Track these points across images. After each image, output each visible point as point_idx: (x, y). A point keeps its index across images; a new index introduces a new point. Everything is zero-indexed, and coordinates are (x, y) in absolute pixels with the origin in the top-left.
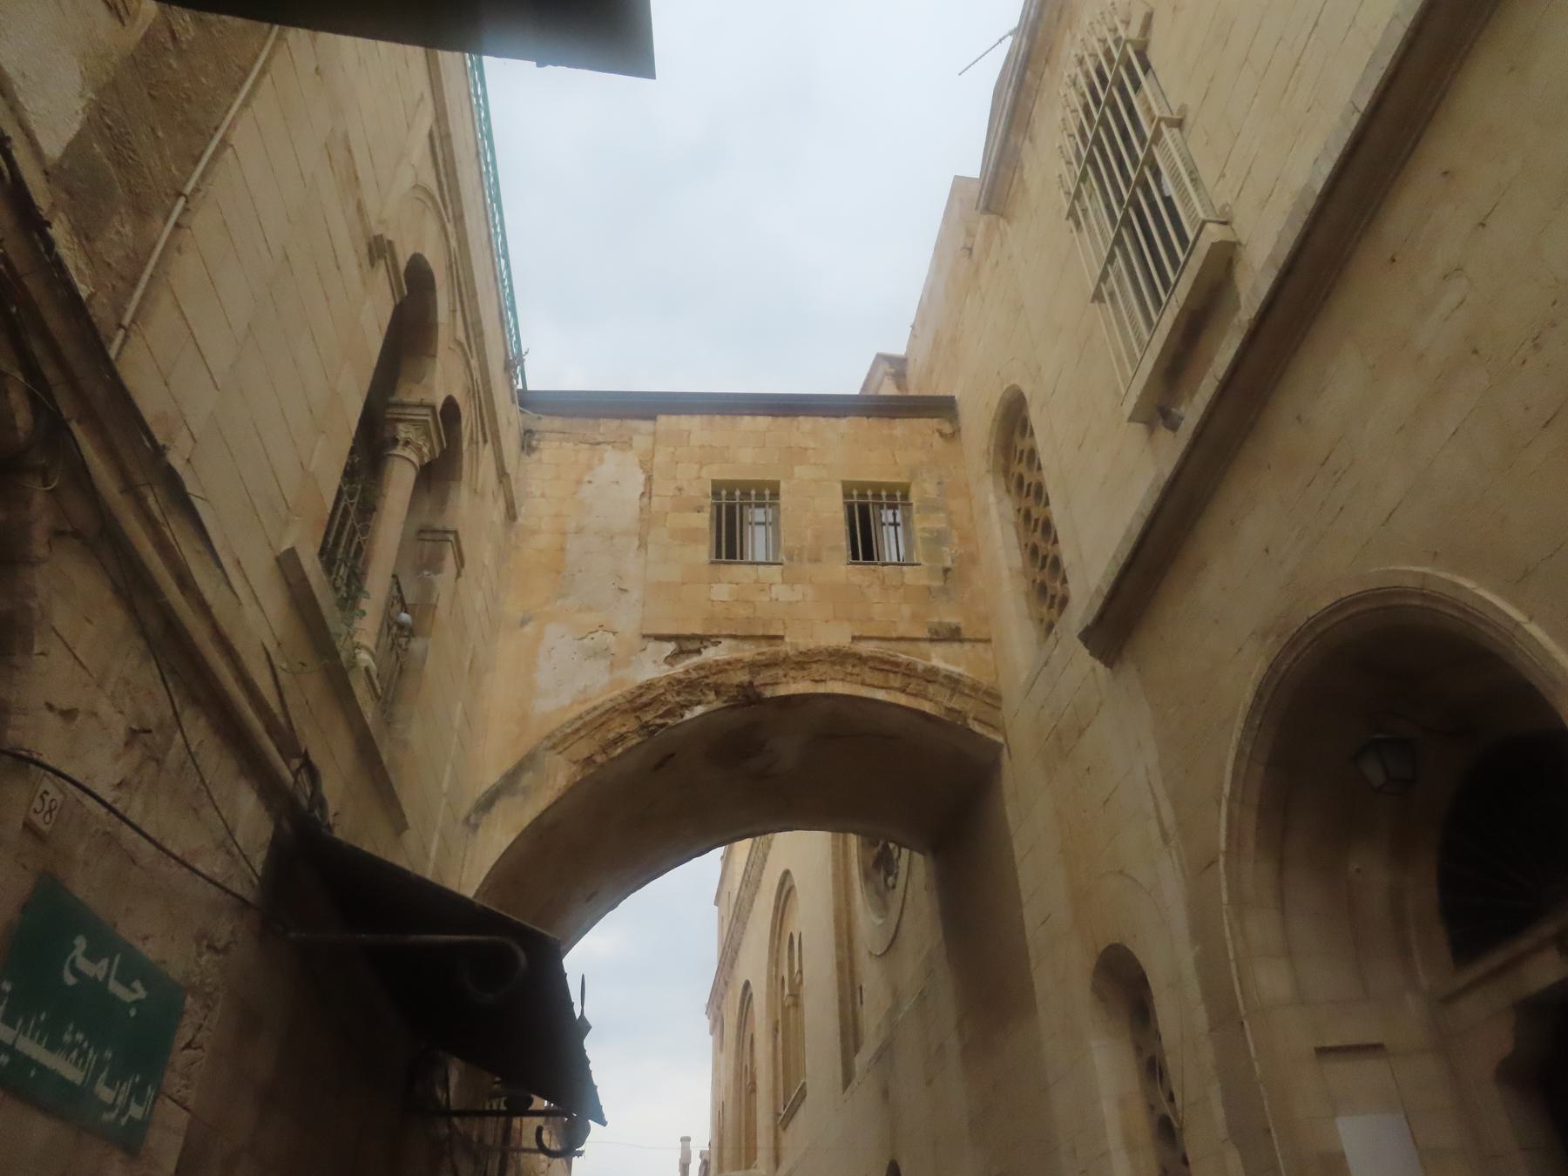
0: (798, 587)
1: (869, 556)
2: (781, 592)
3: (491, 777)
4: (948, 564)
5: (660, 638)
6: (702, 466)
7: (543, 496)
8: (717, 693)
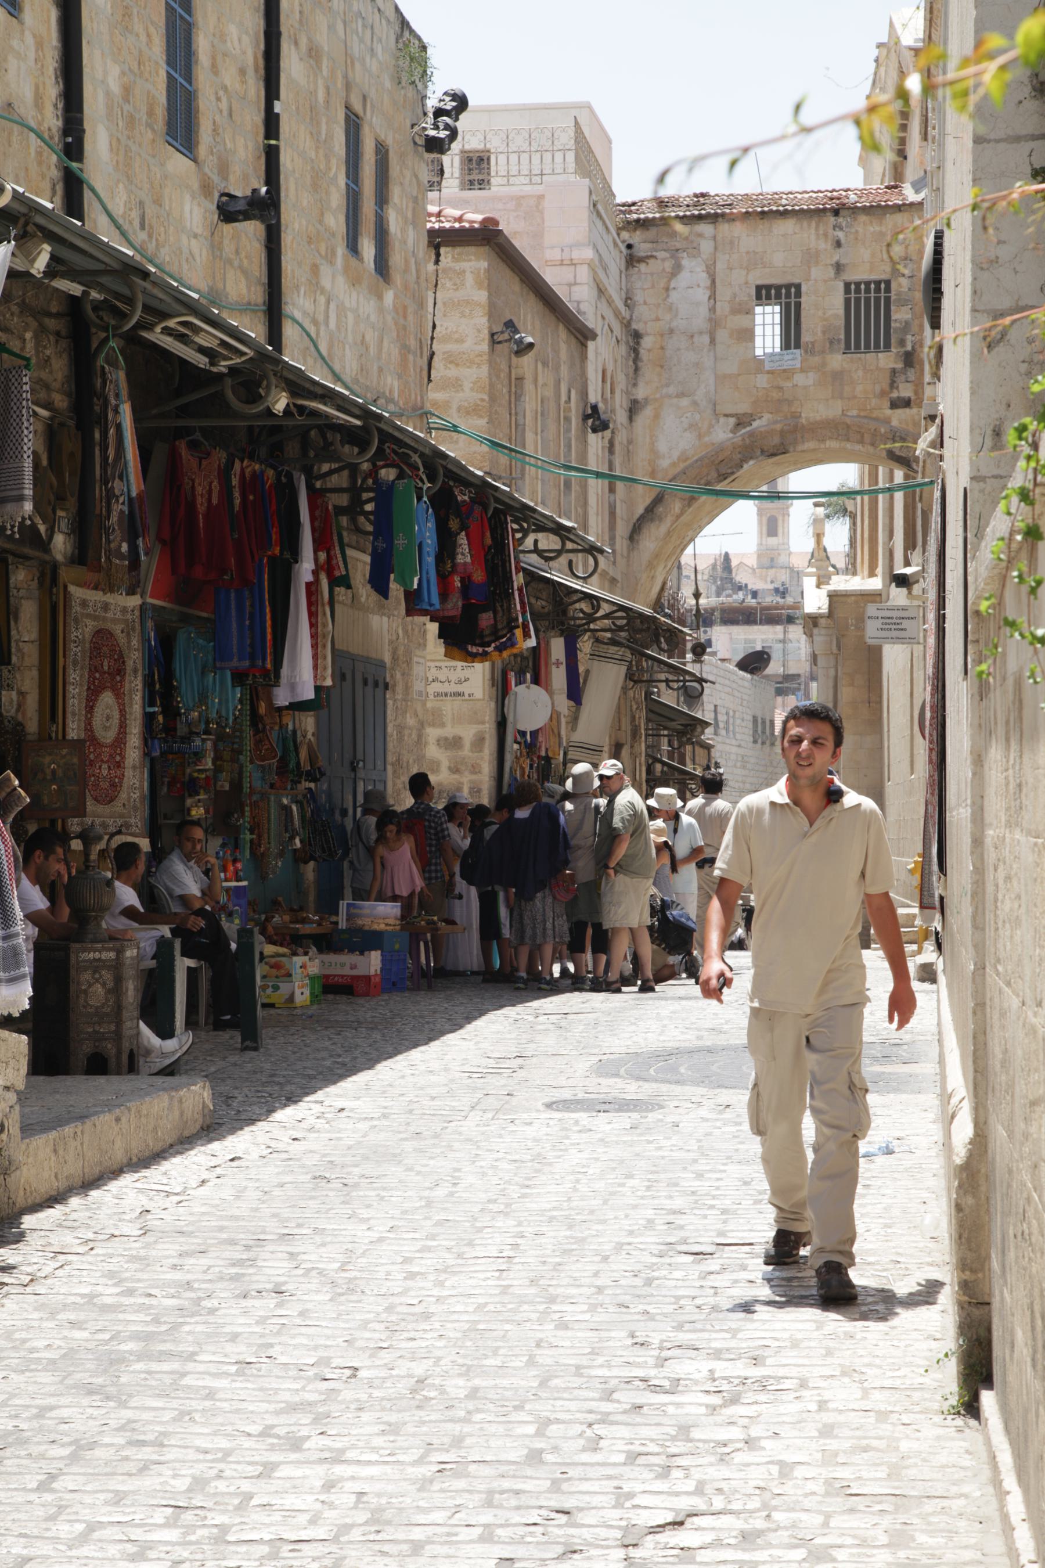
0: (810, 374)
1: (858, 346)
2: (800, 379)
3: (640, 510)
4: (909, 348)
5: (726, 415)
6: (748, 270)
7: (645, 303)
8: (762, 451)
